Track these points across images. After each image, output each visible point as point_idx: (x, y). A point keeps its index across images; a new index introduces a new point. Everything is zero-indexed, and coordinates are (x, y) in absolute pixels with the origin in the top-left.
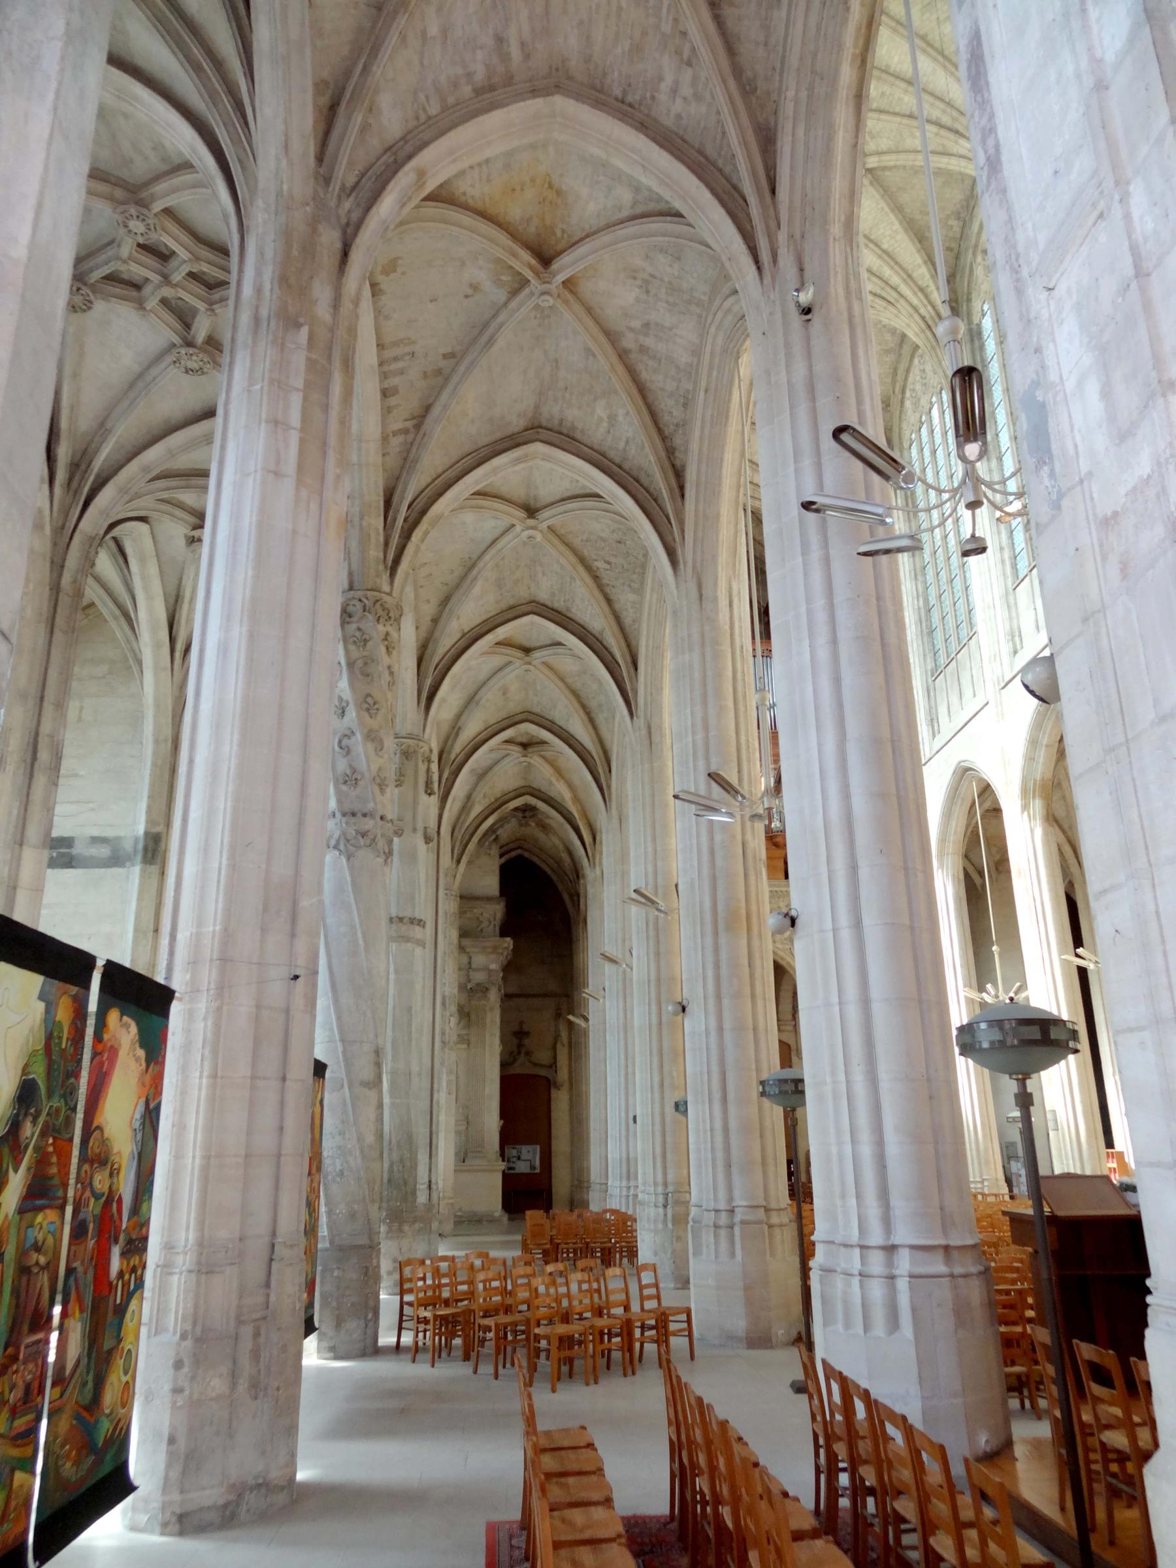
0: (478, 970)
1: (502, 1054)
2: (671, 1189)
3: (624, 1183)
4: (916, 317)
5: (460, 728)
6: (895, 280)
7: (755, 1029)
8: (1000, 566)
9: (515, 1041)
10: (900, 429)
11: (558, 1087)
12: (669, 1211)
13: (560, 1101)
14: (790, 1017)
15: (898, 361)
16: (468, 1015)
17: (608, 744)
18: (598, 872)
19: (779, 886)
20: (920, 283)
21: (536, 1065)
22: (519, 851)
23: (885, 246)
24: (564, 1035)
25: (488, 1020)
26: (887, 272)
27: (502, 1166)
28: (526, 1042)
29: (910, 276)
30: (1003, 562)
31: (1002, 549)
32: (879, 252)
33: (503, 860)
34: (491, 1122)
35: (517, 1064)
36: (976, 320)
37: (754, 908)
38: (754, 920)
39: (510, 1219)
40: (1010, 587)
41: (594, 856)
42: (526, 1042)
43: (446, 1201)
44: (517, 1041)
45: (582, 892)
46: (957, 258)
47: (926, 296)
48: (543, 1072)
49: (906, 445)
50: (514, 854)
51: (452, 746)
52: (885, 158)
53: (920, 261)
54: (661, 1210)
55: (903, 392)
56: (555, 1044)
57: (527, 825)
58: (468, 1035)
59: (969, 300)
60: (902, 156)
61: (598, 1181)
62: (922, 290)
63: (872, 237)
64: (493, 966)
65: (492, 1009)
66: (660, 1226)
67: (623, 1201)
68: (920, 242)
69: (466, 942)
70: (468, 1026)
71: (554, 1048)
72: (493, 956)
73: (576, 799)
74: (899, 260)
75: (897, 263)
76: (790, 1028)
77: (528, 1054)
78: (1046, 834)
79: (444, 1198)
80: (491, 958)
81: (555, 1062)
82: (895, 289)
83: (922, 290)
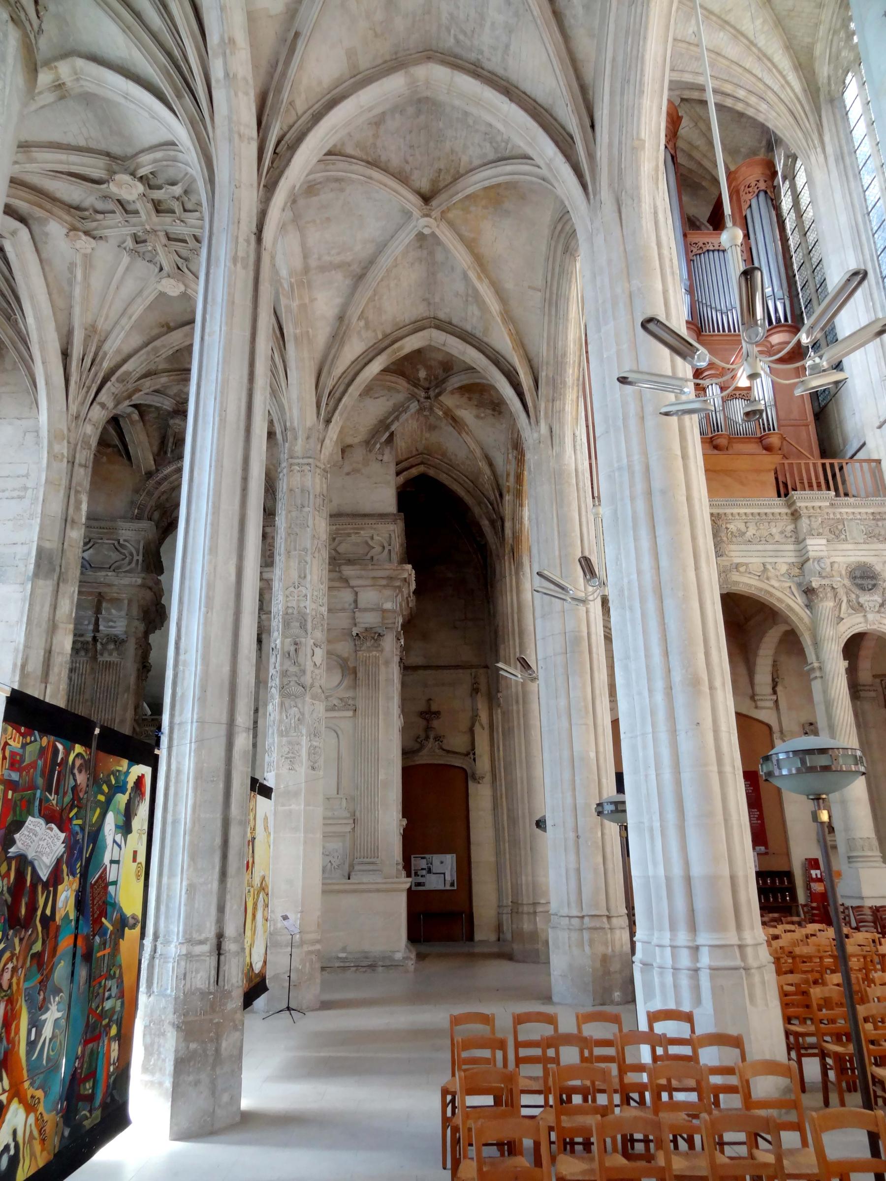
0: (366, 610)
1: (404, 730)
3: (683, 938)
5: (297, 35)
9: (423, 723)
11: (477, 779)
13: (481, 797)
14: (770, 691)
16: (355, 672)
17: (588, 74)
18: (544, 428)
19: (770, 506)
21: (448, 752)
22: (422, 469)
24: (484, 716)
25: (382, 677)
27: (406, 883)
28: (435, 723)
33: (401, 479)
34: (389, 821)
35: (425, 751)
39: (421, 957)
41: (535, 407)
42: (435, 723)
43: (306, 948)
44: (422, 722)
45: (507, 511)
48: (457, 762)
50: (414, 472)
51: (284, 74)
56: (473, 725)
57: (432, 428)
58: (354, 699)
61: (565, 911)
64: (388, 606)
65: (387, 663)
67: (685, 982)
69: (348, 571)
70: (355, 685)
71: (472, 731)
72: (388, 592)
73: (508, 317)
76: (770, 704)
77: (438, 738)
79: (302, 943)
80: (386, 595)
81: (473, 748)
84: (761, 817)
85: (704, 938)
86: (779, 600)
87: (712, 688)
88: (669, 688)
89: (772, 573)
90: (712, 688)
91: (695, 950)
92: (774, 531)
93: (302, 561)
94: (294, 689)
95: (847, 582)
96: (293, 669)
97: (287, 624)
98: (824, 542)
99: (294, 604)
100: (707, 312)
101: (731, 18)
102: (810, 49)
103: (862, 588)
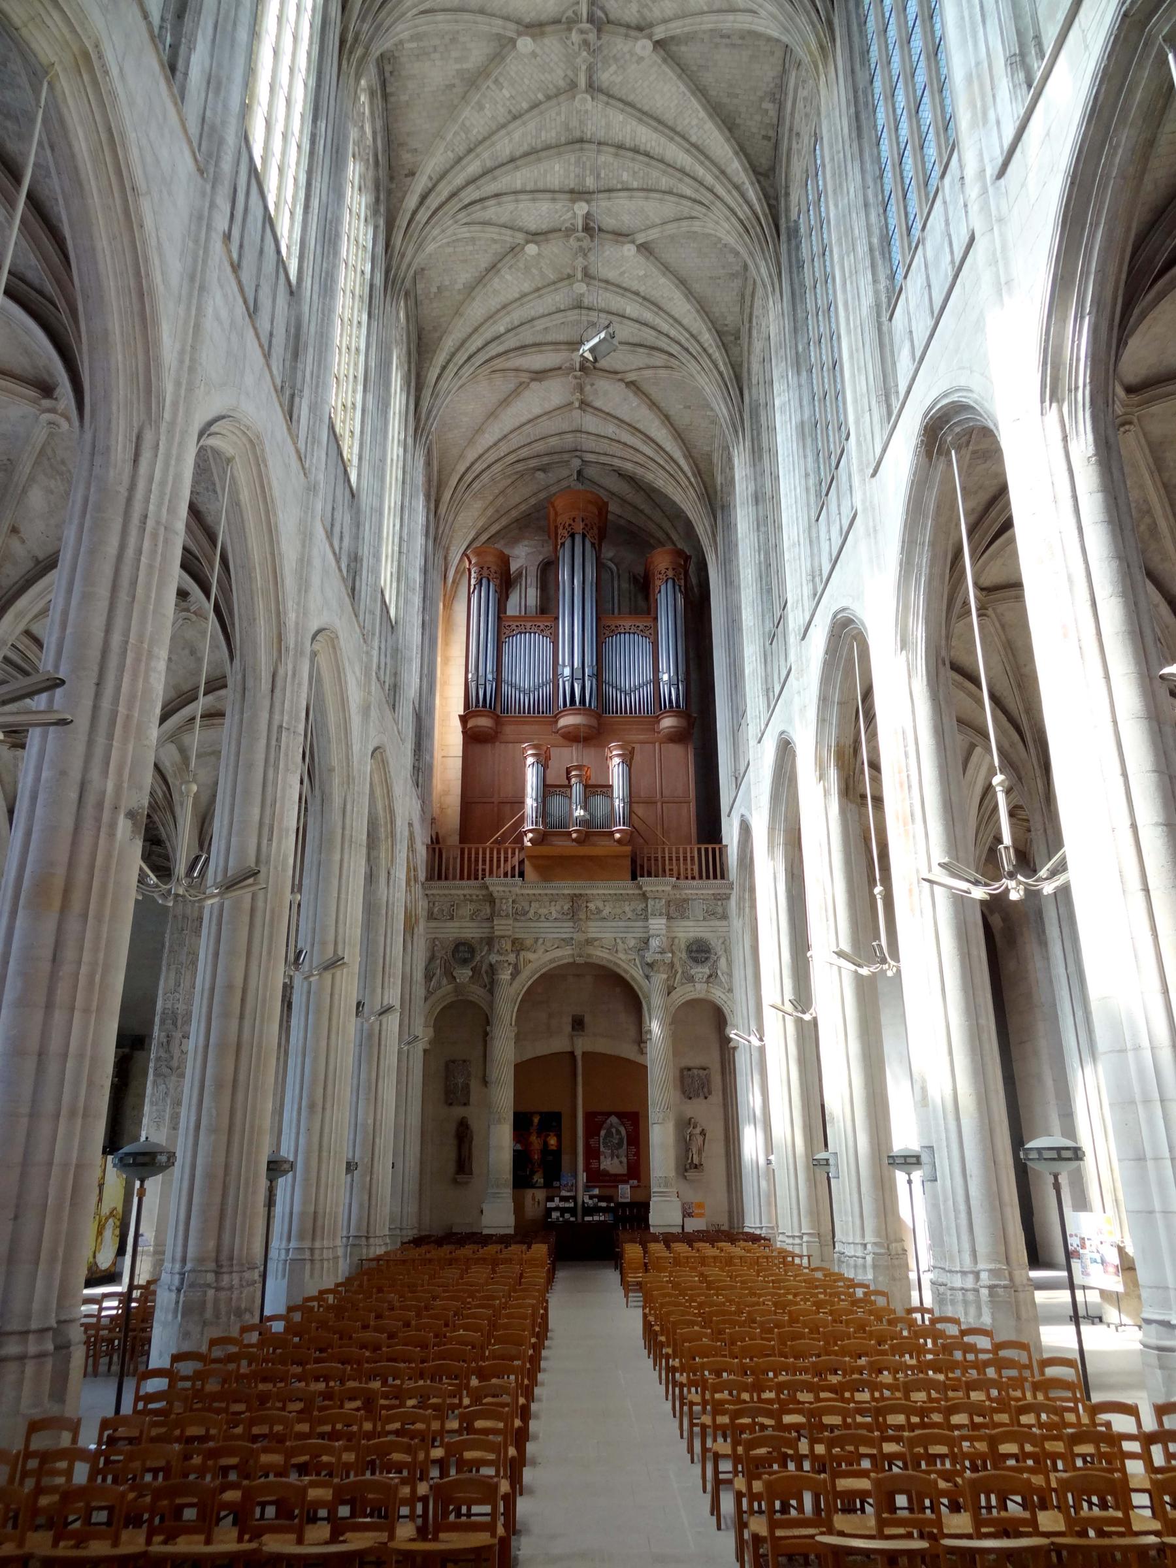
2: (189, 1266)
4: (734, 220)
6: (709, 180)
7: (41, 1054)
8: (804, 495)
10: (749, 363)
12: (182, 1298)
15: (745, 287)
20: (735, 179)
23: (694, 139)
26: (700, 172)
29: (723, 172)
30: (807, 489)
31: (807, 475)
32: (687, 146)
36: (794, 216)
37: (81, 875)
38: (77, 896)
40: (813, 518)
46: (776, 147)
47: (743, 195)
49: (754, 381)
52: (672, 25)
53: (731, 154)
54: (174, 1295)
55: (750, 321)
59: (787, 194)
60: (688, 21)
62: (737, 187)
63: (679, 129)
66: (170, 1317)
68: (730, 130)
74: (711, 155)
75: (707, 157)
78: (843, 811)
82: (711, 190)
83: (737, 187)
84: (637, 1154)
85: (293, 1245)
86: (626, 971)
87: (324, 1109)
88: (300, 1108)
89: (621, 946)
90: (324, 1109)
91: (288, 1250)
92: (627, 909)
93: (178, 972)
94: (165, 1070)
95: (684, 955)
96: (164, 1055)
97: (163, 1022)
98: (664, 921)
99: (169, 1006)
100: (611, 692)
101: (640, 426)
102: (709, 457)
103: (696, 961)
